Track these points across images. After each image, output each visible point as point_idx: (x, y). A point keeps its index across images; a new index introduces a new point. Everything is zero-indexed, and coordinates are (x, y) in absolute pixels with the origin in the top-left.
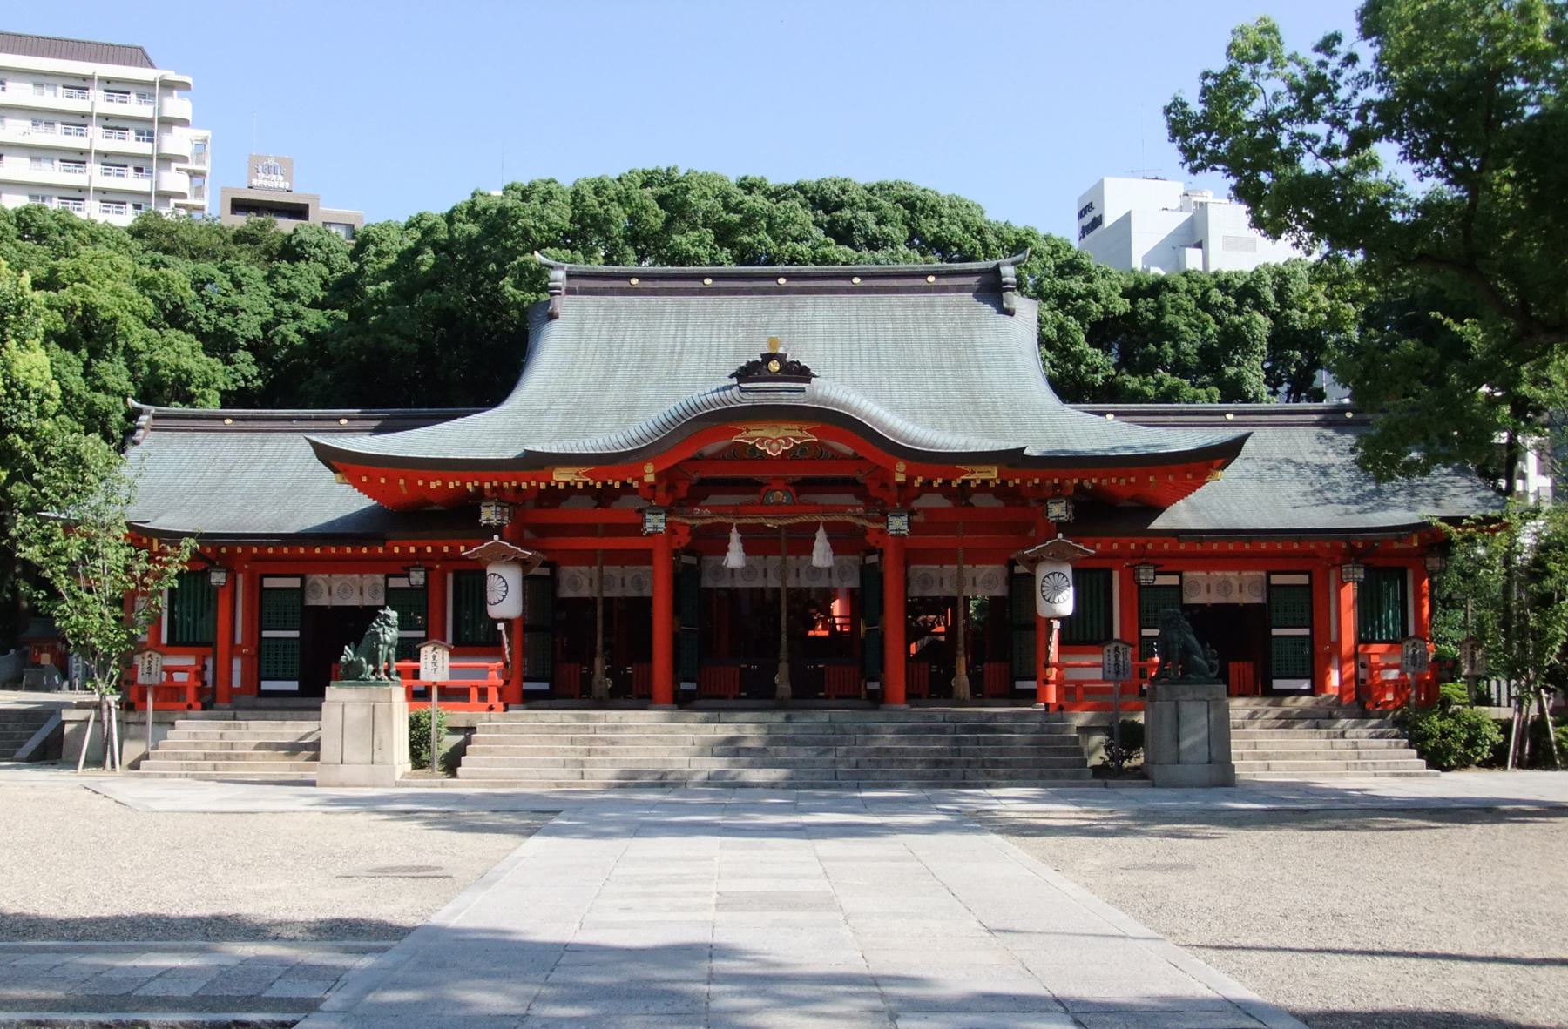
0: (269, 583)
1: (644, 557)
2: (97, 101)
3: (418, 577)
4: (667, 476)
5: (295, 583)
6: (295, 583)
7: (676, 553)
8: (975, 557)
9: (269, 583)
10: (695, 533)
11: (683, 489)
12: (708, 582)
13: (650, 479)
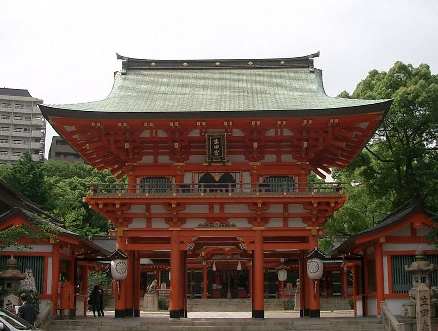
2: (12, 109)
3: (155, 272)
7: (208, 268)
11: (209, 257)
13: (203, 255)
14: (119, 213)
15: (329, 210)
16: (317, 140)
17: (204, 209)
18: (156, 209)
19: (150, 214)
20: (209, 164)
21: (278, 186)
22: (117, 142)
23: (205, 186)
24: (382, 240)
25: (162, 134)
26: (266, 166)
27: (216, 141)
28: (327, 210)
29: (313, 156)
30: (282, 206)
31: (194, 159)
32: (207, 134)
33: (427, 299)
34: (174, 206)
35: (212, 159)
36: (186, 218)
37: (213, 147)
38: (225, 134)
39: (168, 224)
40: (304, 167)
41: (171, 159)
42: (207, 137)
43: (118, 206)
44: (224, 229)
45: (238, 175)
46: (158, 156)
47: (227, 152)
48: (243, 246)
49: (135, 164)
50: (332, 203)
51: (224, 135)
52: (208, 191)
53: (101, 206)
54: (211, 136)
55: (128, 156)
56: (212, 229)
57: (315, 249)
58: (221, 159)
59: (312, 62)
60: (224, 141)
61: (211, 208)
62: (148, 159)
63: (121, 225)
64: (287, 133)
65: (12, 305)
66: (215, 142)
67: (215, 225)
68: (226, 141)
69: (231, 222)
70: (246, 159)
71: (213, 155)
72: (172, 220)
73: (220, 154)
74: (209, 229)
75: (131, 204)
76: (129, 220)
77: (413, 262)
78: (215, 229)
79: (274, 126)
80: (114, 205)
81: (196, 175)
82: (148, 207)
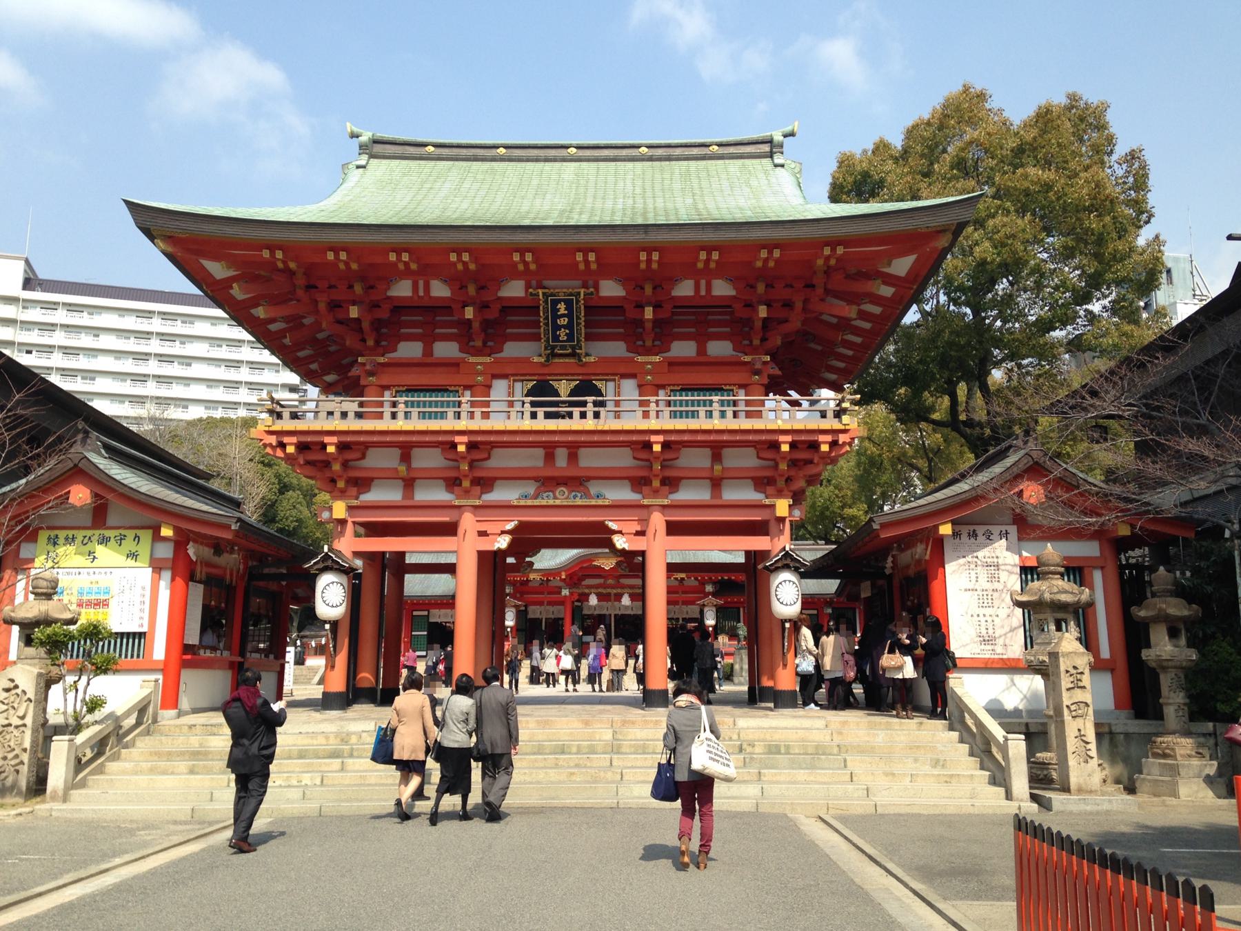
0: (415, 613)
1: (562, 602)
4: (570, 576)
5: (426, 613)
6: (426, 613)
8: (686, 603)
9: (415, 613)
10: (580, 595)
12: (585, 612)
13: (563, 577)
14: (336, 467)
15: (815, 461)
16: (788, 305)
17: (533, 459)
18: (427, 459)
19: (409, 468)
20: (547, 360)
21: (699, 406)
22: (335, 306)
23: (533, 404)
24: (946, 529)
25: (440, 290)
26: (673, 364)
27: (562, 308)
28: (811, 462)
29: (779, 342)
30: (708, 451)
31: (512, 350)
32: (540, 292)
33: (1082, 673)
34: (461, 448)
35: (553, 348)
36: (495, 479)
37: (554, 322)
38: (582, 291)
39: (453, 493)
40: (758, 366)
41: (461, 350)
42: (541, 297)
43: (331, 449)
44: (579, 502)
45: (611, 385)
46: (433, 342)
47: (586, 334)
48: (620, 542)
49: (381, 360)
50: (825, 443)
51: (579, 293)
52: (541, 414)
53: (291, 449)
54: (552, 295)
55: (364, 340)
56: (551, 502)
57: (784, 548)
58: (573, 348)
59: (781, 146)
60: (578, 309)
61: (550, 457)
62: (410, 350)
63: (342, 495)
64: (722, 288)
65: (19, 691)
66: (558, 310)
67: (557, 494)
68: (582, 307)
69: (594, 488)
70: (628, 351)
71: (556, 338)
72: (460, 485)
73: (570, 337)
74: (544, 502)
75: (367, 446)
76: (362, 483)
77: (1033, 580)
78: (558, 502)
79: (691, 271)
80: (324, 446)
81: (518, 386)
82: (406, 458)
